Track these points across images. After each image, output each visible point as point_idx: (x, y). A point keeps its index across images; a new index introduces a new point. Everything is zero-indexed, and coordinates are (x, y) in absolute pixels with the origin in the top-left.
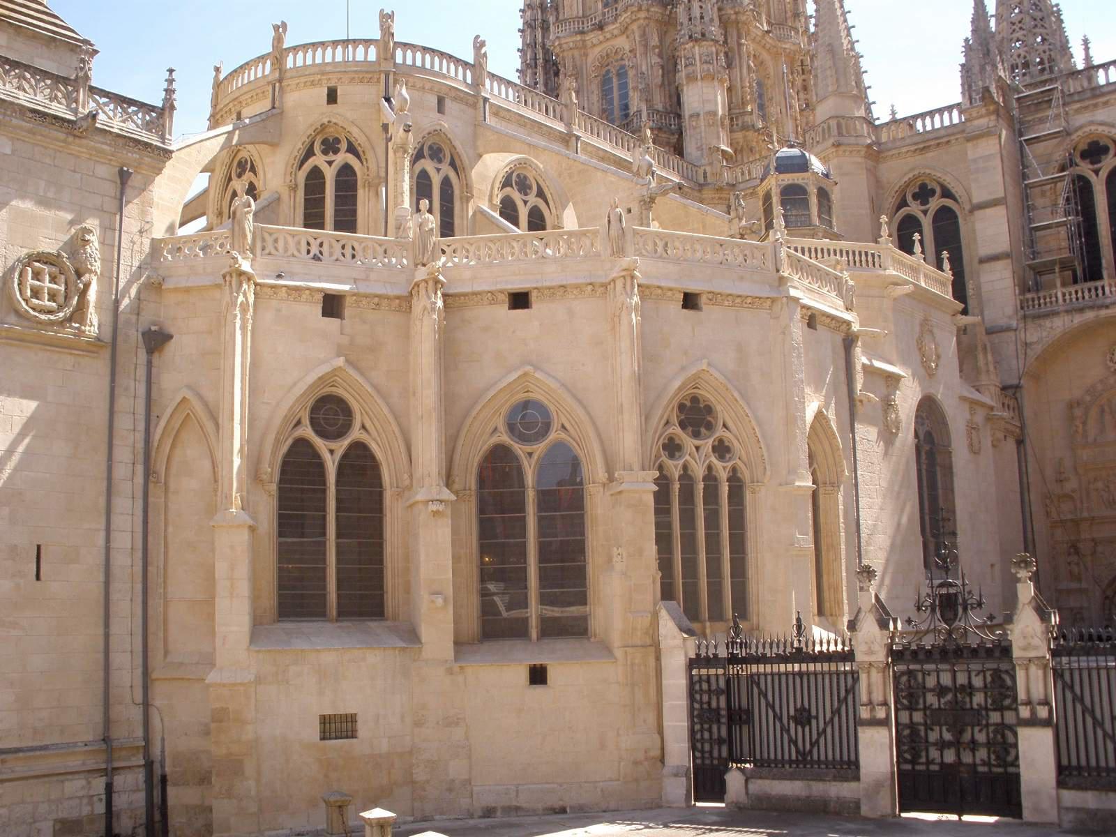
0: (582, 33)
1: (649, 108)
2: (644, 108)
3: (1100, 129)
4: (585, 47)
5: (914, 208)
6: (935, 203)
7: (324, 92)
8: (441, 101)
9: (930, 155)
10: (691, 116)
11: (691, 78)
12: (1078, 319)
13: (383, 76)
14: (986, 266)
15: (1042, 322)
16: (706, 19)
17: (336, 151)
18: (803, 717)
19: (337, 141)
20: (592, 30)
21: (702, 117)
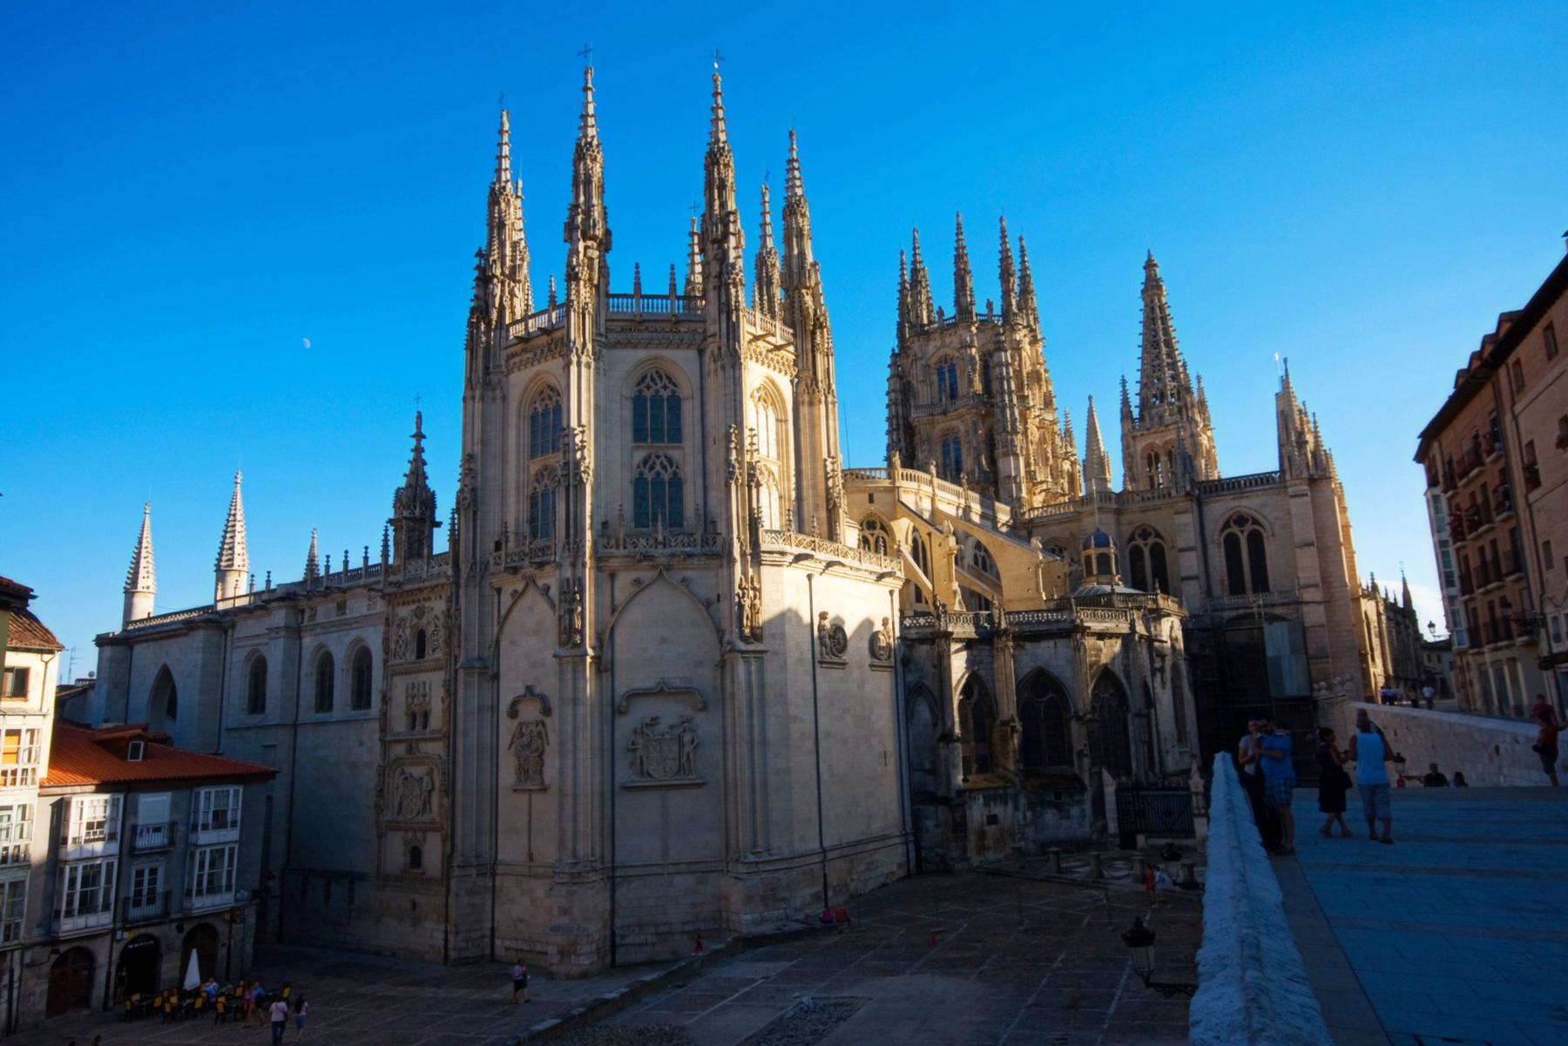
0: (932, 415)
1: (979, 468)
4: (933, 423)
6: (1151, 540)
9: (1150, 514)
14: (1185, 582)
17: (875, 528)
18: (1168, 813)
19: (874, 522)
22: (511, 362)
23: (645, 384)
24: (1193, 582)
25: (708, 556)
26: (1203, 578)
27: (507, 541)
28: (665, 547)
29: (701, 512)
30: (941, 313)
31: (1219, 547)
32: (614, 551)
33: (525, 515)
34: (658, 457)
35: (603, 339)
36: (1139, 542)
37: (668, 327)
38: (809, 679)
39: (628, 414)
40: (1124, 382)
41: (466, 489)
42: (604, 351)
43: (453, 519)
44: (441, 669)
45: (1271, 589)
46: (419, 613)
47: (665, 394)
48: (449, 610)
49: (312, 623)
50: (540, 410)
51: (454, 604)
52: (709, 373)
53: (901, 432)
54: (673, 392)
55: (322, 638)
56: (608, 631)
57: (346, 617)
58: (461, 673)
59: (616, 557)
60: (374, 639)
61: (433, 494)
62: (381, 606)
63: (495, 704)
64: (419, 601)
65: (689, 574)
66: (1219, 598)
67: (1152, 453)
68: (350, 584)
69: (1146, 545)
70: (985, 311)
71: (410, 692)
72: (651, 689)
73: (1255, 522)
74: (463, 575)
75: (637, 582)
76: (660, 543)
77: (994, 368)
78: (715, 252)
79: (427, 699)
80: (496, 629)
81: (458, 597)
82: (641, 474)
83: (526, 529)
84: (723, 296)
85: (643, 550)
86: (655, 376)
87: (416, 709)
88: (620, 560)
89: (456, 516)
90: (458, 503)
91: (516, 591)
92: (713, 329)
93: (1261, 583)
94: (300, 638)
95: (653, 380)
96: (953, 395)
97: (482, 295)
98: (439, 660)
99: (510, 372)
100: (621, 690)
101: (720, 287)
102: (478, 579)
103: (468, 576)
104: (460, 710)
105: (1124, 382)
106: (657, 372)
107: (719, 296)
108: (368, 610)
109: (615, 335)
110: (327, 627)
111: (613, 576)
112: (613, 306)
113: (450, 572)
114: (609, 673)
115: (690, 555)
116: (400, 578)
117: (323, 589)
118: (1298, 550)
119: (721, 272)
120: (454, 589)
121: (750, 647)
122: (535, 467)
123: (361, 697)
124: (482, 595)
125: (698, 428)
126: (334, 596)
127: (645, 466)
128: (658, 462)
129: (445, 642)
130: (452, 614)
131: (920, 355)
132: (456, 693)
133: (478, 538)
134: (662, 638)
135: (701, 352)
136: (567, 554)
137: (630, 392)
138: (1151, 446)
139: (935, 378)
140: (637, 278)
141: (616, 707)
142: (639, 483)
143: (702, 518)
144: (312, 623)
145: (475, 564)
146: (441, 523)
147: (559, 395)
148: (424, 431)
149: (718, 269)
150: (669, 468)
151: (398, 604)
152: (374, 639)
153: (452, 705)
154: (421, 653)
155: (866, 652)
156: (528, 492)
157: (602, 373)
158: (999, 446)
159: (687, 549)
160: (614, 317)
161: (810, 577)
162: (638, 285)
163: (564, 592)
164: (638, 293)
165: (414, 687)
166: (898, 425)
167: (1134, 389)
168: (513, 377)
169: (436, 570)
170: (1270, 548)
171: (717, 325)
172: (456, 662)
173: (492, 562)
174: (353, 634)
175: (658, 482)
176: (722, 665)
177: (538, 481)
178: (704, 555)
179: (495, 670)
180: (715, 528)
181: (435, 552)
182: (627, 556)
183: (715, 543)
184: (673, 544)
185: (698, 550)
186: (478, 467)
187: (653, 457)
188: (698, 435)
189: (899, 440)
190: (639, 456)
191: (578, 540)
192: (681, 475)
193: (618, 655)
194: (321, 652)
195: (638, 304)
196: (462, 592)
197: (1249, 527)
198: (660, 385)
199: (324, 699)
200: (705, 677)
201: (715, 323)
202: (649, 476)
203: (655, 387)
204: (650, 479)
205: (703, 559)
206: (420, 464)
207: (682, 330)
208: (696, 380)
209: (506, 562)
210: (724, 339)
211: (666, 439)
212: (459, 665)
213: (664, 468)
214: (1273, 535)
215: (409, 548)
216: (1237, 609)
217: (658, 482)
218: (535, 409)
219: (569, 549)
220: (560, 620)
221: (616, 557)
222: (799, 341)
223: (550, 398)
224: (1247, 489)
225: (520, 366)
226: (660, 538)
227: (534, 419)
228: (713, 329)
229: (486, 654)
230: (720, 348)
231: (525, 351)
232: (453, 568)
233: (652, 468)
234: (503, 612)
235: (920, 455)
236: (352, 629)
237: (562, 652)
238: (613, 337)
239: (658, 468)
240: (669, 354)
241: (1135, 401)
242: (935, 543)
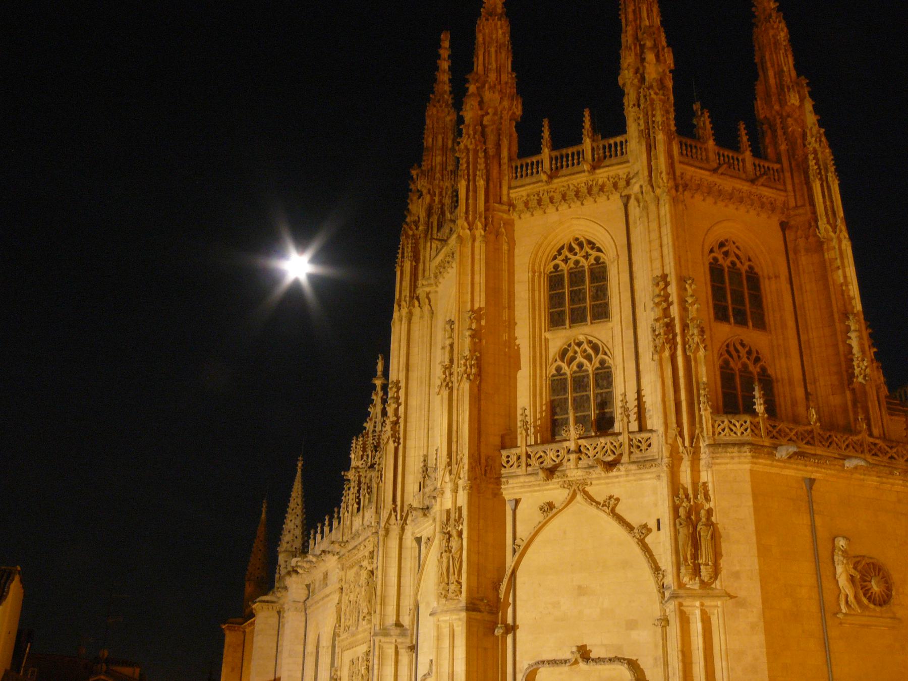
23: (562, 257)
54: (597, 259)
59: (517, 476)
82: (559, 369)
91: (429, 539)
95: (571, 249)
125: (627, 295)
134: (580, 587)
136: (447, 478)
145: (395, 510)
183: (649, 445)
184: (591, 453)
187: (573, 344)
192: (610, 361)
203: (573, 258)
204: (568, 373)
205: (633, 467)
213: (589, 358)
233: (573, 359)
239: (580, 359)
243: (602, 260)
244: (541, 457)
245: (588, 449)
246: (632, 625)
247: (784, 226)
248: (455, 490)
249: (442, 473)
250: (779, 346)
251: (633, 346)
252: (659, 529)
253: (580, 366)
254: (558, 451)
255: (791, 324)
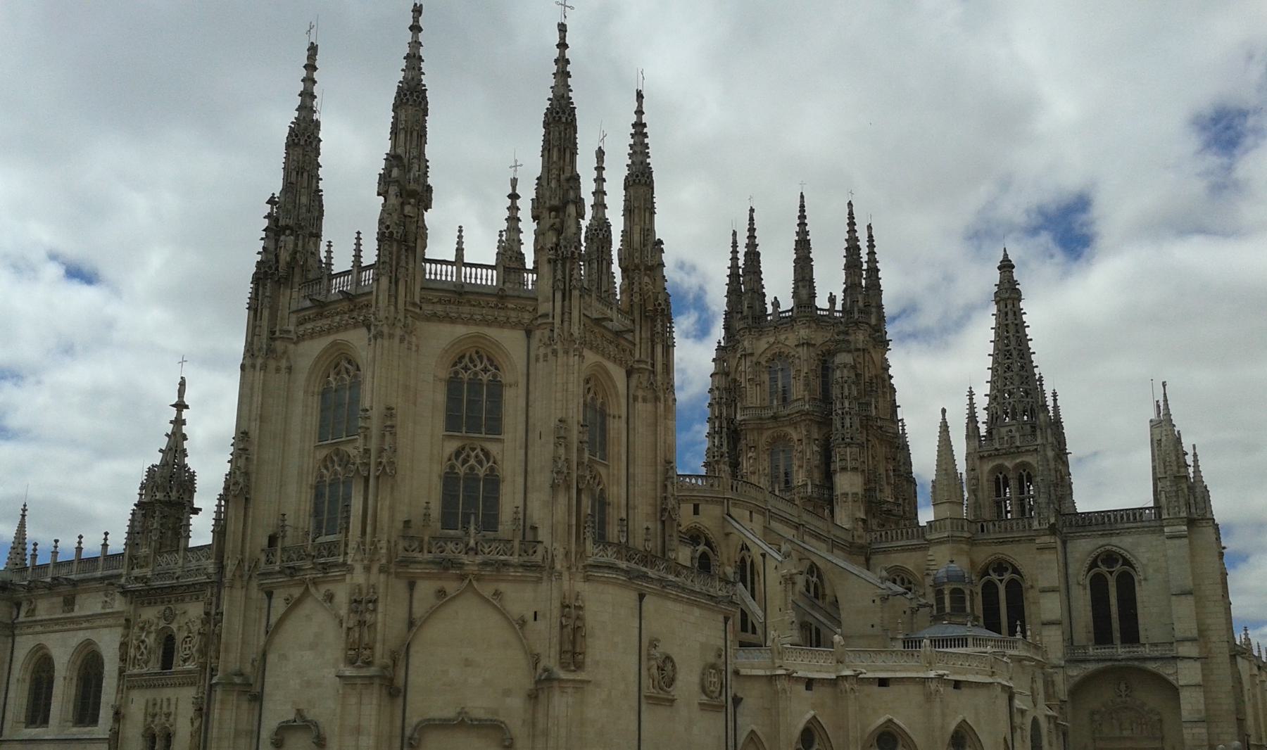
2: (809, 483)
3: (1114, 549)
5: (994, 577)
6: (1007, 576)
7: (692, 506)
8: (751, 512)
10: (842, 494)
11: (844, 469)
12: (1101, 665)
13: (726, 501)
15: (1079, 664)
16: (854, 428)
17: (698, 544)
19: (698, 537)
20: (769, 419)
21: (850, 496)
22: (301, 328)
24: (1054, 627)
25: (524, 566)
26: (1066, 622)
27: (283, 537)
28: (476, 554)
29: (521, 515)
30: (776, 304)
31: (1085, 589)
32: (416, 554)
33: (307, 505)
34: (473, 449)
35: (418, 310)
36: (994, 577)
37: (493, 301)
38: (634, 717)
39: (441, 397)
40: (971, 394)
41: (238, 472)
42: (417, 323)
43: (219, 506)
44: (192, 684)
45: (1142, 640)
46: (169, 617)
47: (485, 378)
48: (207, 614)
49: (30, 619)
50: (334, 385)
51: (214, 608)
52: (537, 360)
53: (724, 435)
54: (495, 376)
55: (43, 639)
56: (404, 649)
57: (73, 614)
58: (219, 689)
59: (420, 562)
60: (108, 643)
61: (192, 475)
62: (119, 604)
63: (255, 728)
64: (169, 602)
65: (502, 587)
66: (1084, 647)
67: (1001, 476)
68: (82, 576)
69: (1001, 581)
70: (827, 306)
71: (150, 710)
72: (449, 720)
73: (1126, 562)
74: (229, 575)
75: (441, 593)
76: (472, 549)
77: (833, 370)
78: (552, 221)
79: (171, 719)
80: (263, 639)
81: (218, 599)
82: (452, 467)
83: (307, 523)
84: (559, 272)
85: (451, 556)
86: (475, 357)
87: (157, 730)
88: (423, 566)
89: (223, 503)
90: (226, 488)
92: (544, 307)
93: (1131, 635)
94: (13, 636)
95: (472, 360)
96: (784, 399)
97: (272, 247)
98: (190, 672)
99: (301, 339)
100: (413, 719)
101: (555, 261)
102: (246, 577)
103: (234, 575)
104: (214, 732)
105: (971, 394)
106: (477, 352)
107: (555, 271)
108: (103, 608)
109: (431, 307)
110: (50, 624)
111: (412, 586)
112: (430, 273)
113: (211, 569)
114: (400, 700)
115: (506, 564)
116: (148, 572)
117: (49, 580)
118: (1174, 598)
119: (557, 245)
120: (215, 590)
121: (570, 676)
122: (325, 452)
123: (86, 711)
124: (247, 597)
125: (522, 418)
126: (62, 589)
127: (457, 459)
128: (473, 454)
129: (200, 651)
130: (212, 618)
131: (749, 351)
132: (208, 715)
133: (249, 532)
134: (466, 660)
135: (529, 333)
137: (444, 374)
138: (999, 468)
139: (766, 377)
140: (460, 243)
141: (406, 741)
142: (449, 479)
143: (521, 522)
144: (30, 619)
145: (242, 560)
146: (200, 510)
147: (358, 369)
148: (187, 400)
149: (554, 240)
150: (485, 462)
151: (142, 603)
152: (108, 643)
153: (203, 727)
154: (167, 662)
155: (696, 688)
156: (312, 480)
157: (414, 348)
158: (837, 458)
159: (502, 558)
160: (431, 285)
161: (641, 597)
162: (460, 251)
163: (355, 601)
164: (459, 261)
165: (155, 704)
166: (721, 427)
167: (982, 401)
168: (306, 346)
169: (193, 564)
170: (1144, 594)
171: (551, 303)
172: (212, 677)
173: (263, 558)
174: (81, 636)
175: (472, 478)
176: (533, 697)
177: (327, 468)
178: (522, 566)
179: (259, 690)
180: (536, 535)
181: (192, 543)
182: (428, 562)
183: (535, 552)
184: (487, 550)
185: (515, 559)
186: (254, 449)
187: (467, 449)
188: (522, 427)
189: (722, 445)
190: (452, 446)
191: (376, 539)
193: (412, 678)
194: (40, 653)
195: (459, 272)
196: (225, 593)
197: (1118, 568)
198: (479, 367)
199: (38, 712)
200: (514, 710)
201: (549, 301)
202: (462, 470)
204: (462, 474)
206: (179, 438)
207: (510, 306)
208: (521, 366)
209: (283, 561)
210: (557, 320)
211: (483, 429)
212: (214, 682)
213: (480, 463)
214: (1145, 579)
215: (161, 537)
216: (1105, 660)
217: (472, 478)
218: (328, 383)
219: (364, 550)
220: (348, 635)
221: (420, 562)
222: (638, 327)
223: (348, 372)
224: (1119, 526)
225: (312, 335)
226: (472, 543)
227: (324, 394)
228: (544, 307)
229: (248, 669)
230: (552, 331)
231: (320, 316)
232: (215, 563)
233: (465, 461)
234: (273, 620)
235: (746, 465)
236: (80, 629)
237: (349, 671)
238: (428, 308)
239: (472, 462)
240: (493, 333)
241: (982, 416)
242: (771, 564)
243: (499, 379)
244: (440, 547)
245: (484, 547)
246: (507, 693)
247: (629, 374)
248: (367, 569)
249: (353, 552)
250: (614, 475)
251: (523, 464)
252: (535, 619)
253: (472, 468)
254: (457, 544)
255: (624, 458)
